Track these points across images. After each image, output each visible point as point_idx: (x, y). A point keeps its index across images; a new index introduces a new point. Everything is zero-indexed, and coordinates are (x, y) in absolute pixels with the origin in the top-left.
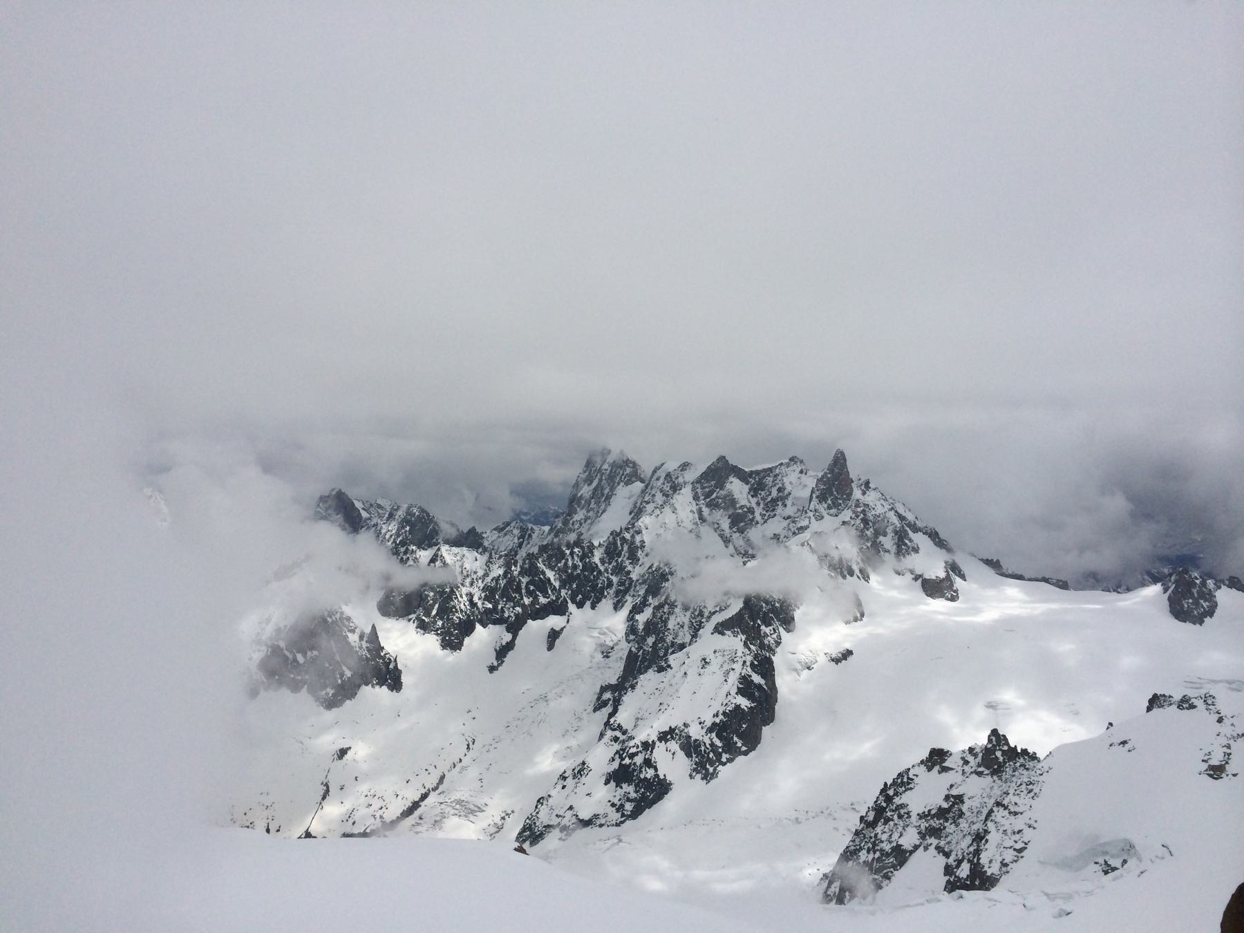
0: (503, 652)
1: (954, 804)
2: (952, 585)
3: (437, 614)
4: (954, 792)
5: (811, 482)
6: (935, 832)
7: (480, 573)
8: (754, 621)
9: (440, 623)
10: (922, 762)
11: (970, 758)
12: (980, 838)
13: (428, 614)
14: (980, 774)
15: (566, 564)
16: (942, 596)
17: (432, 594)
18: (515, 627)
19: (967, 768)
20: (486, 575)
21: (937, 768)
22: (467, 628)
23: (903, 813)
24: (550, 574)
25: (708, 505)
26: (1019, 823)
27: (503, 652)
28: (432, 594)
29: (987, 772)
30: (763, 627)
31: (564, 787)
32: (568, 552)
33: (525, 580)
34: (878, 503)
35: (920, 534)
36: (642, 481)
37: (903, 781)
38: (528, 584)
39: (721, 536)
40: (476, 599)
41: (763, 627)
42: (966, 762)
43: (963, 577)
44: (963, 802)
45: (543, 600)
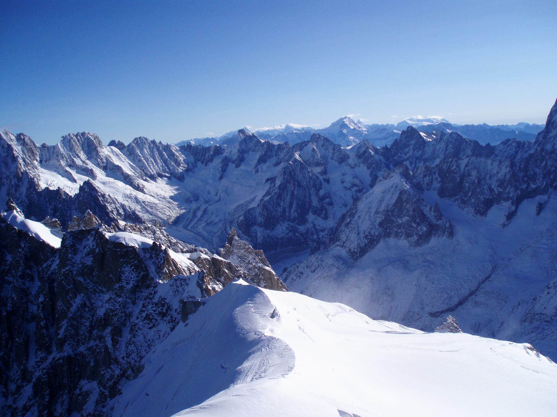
0: (510, 216)
3: (471, 196)
7: (495, 172)
9: (473, 200)
13: (466, 196)
15: (546, 164)
17: (467, 184)
18: (518, 202)
20: (498, 172)
22: (489, 204)
24: (537, 170)
27: (510, 216)
28: (467, 184)
31: (548, 293)
32: (547, 157)
33: (522, 174)
38: (523, 176)
40: (493, 187)
45: (533, 186)
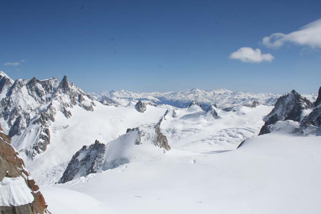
1: (88, 157)
2: (92, 107)
4: (88, 155)
5: (58, 84)
6: (84, 164)
8: (44, 120)
10: (81, 149)
11: (92, 147)
12: (93, 164)
14: (93, 150)
16: (90, 110)
19: (91, 149)
21: (85, 150)
23: (77, 161)
25: (30, 90)
26: (101, 159)
29: (95, 149)
30: (46, 121)
34: (75, 89)
35: (85, 96)
36: (12, 84)
37: (78, 154)
39: (31, 96)
41: (46, 121)
42: (91, 148)
43: (95, 106)
44: (90, 157)
